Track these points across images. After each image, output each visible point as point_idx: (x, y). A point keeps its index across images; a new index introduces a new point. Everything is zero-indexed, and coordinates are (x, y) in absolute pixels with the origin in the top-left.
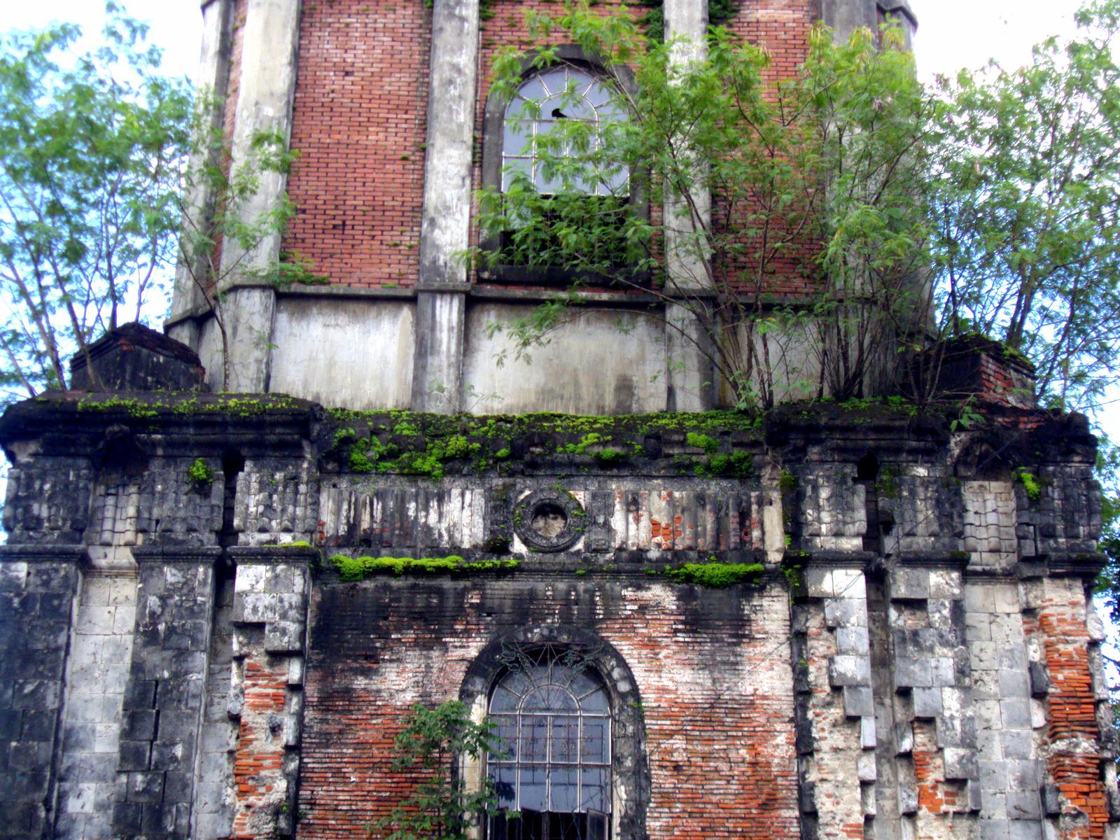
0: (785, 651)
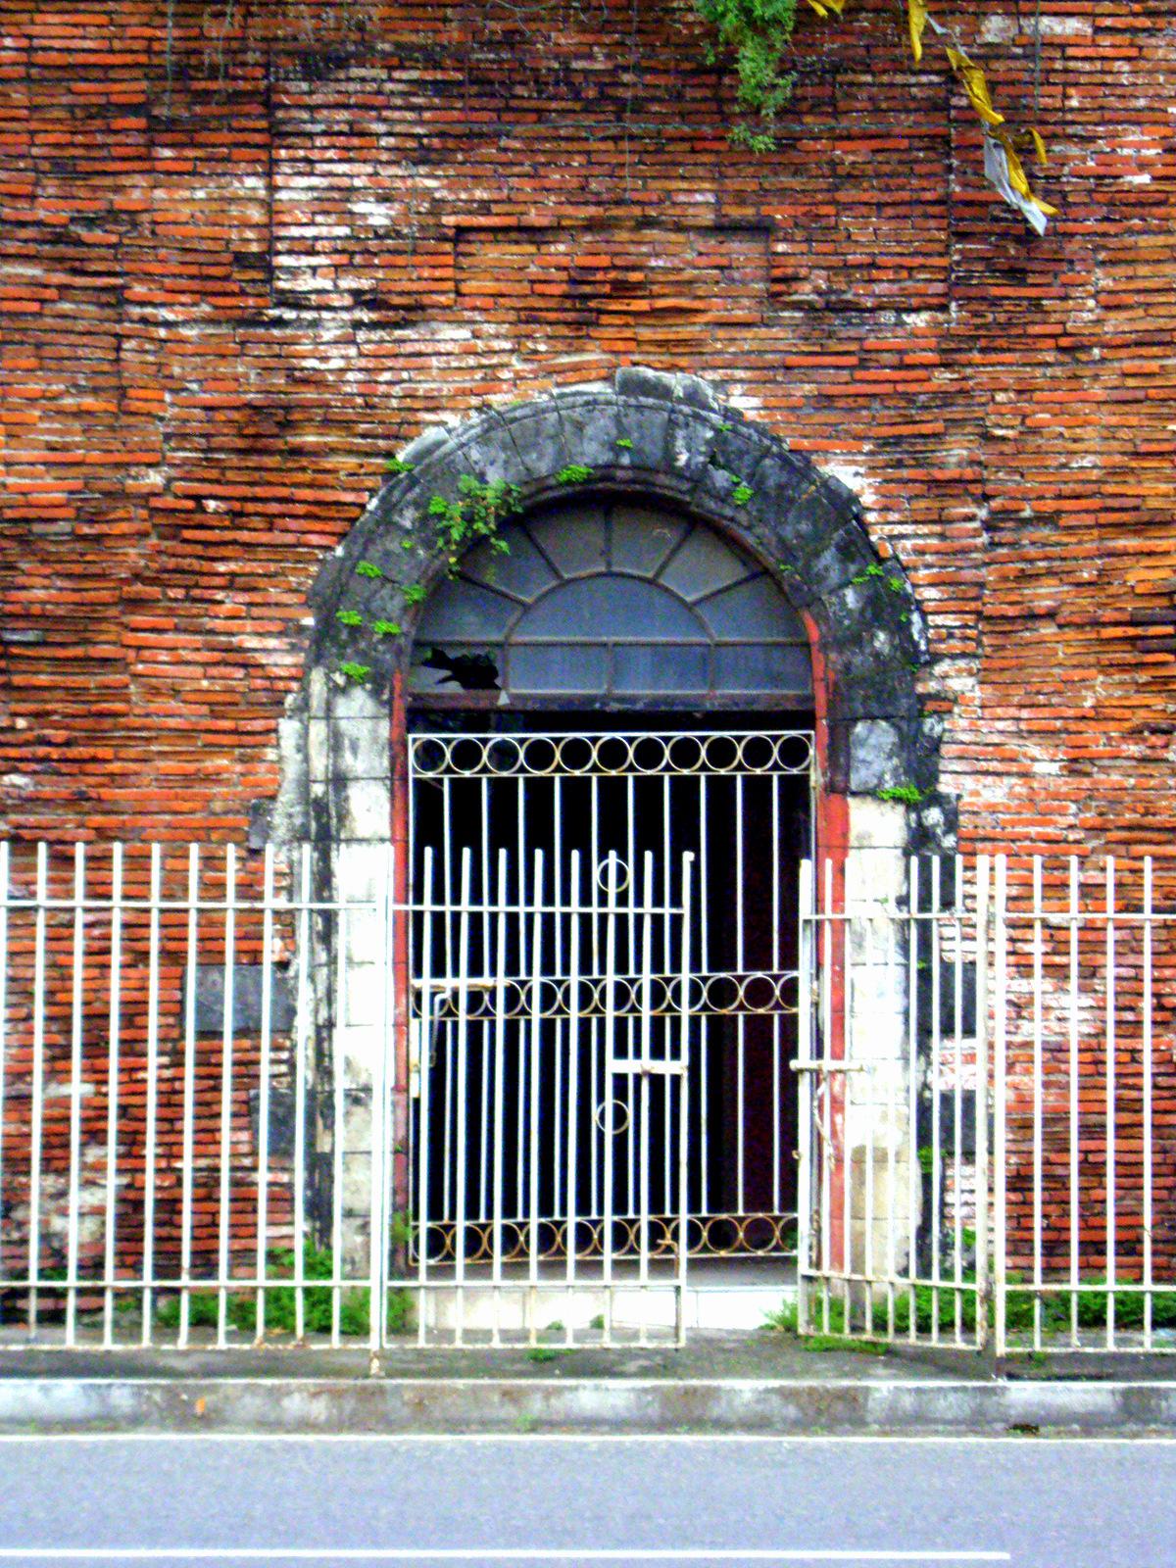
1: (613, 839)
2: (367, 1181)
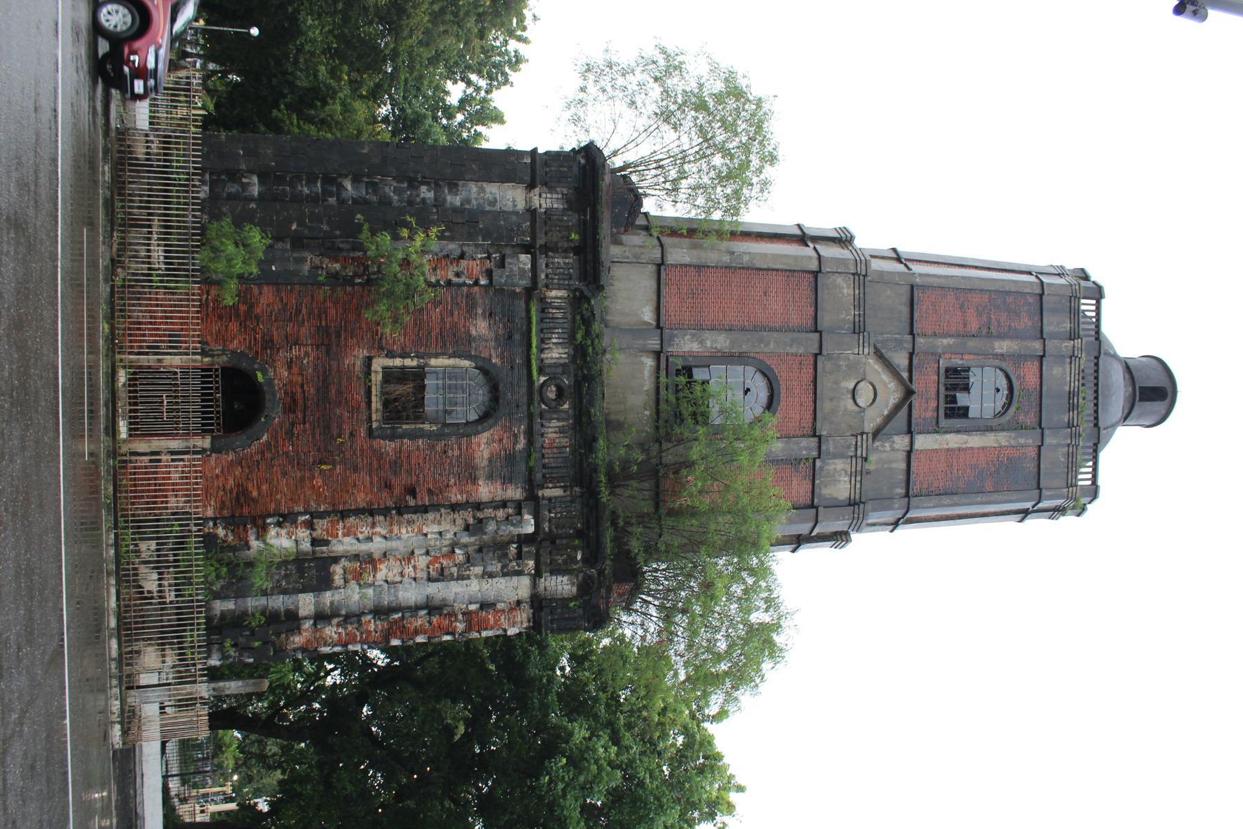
0: (498, 499)
1: (203, 401)
2: (144, 360)
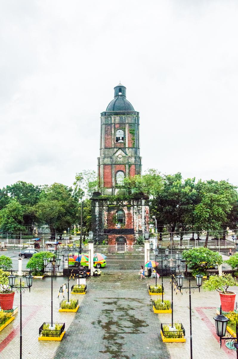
2: (116, 250)
